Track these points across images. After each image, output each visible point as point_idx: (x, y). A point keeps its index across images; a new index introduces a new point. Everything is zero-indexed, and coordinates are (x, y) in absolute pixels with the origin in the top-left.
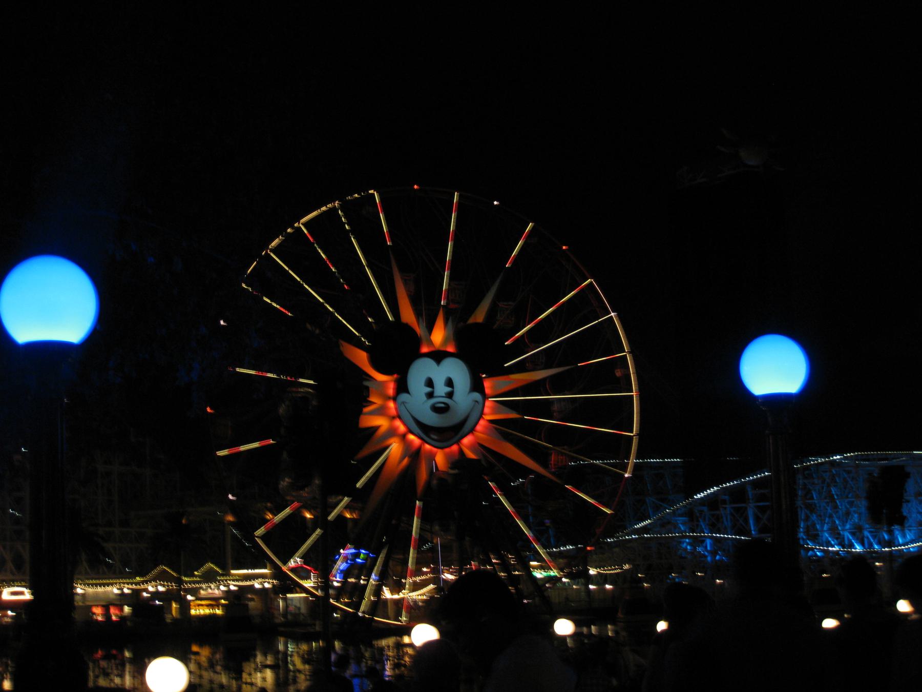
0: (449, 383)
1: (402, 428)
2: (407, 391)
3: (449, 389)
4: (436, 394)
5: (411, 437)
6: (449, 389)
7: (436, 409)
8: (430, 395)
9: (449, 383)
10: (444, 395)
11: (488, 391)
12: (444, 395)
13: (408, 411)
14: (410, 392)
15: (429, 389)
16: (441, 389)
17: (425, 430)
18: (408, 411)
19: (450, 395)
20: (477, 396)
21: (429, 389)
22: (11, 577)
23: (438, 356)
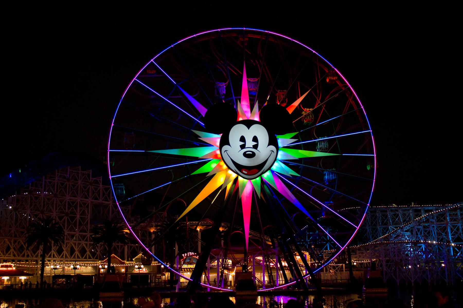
0: (255, 139)
1: (225, 167)
3: (255, 143)
4: (246, 147)
5: (230, 172)
6: (255, 143)
7: (245, 155)
8: (243, 147)
9: (255, 139)
11: (280, 145)
13: (228, 155)
15: (243, 143)
16: (250, 143)
17: (239, 168)
18: (228, 155)
19: (256, 147)
20: (272, 148)
21: (243, 143)
22: (13, 258)
23: (249, 123)
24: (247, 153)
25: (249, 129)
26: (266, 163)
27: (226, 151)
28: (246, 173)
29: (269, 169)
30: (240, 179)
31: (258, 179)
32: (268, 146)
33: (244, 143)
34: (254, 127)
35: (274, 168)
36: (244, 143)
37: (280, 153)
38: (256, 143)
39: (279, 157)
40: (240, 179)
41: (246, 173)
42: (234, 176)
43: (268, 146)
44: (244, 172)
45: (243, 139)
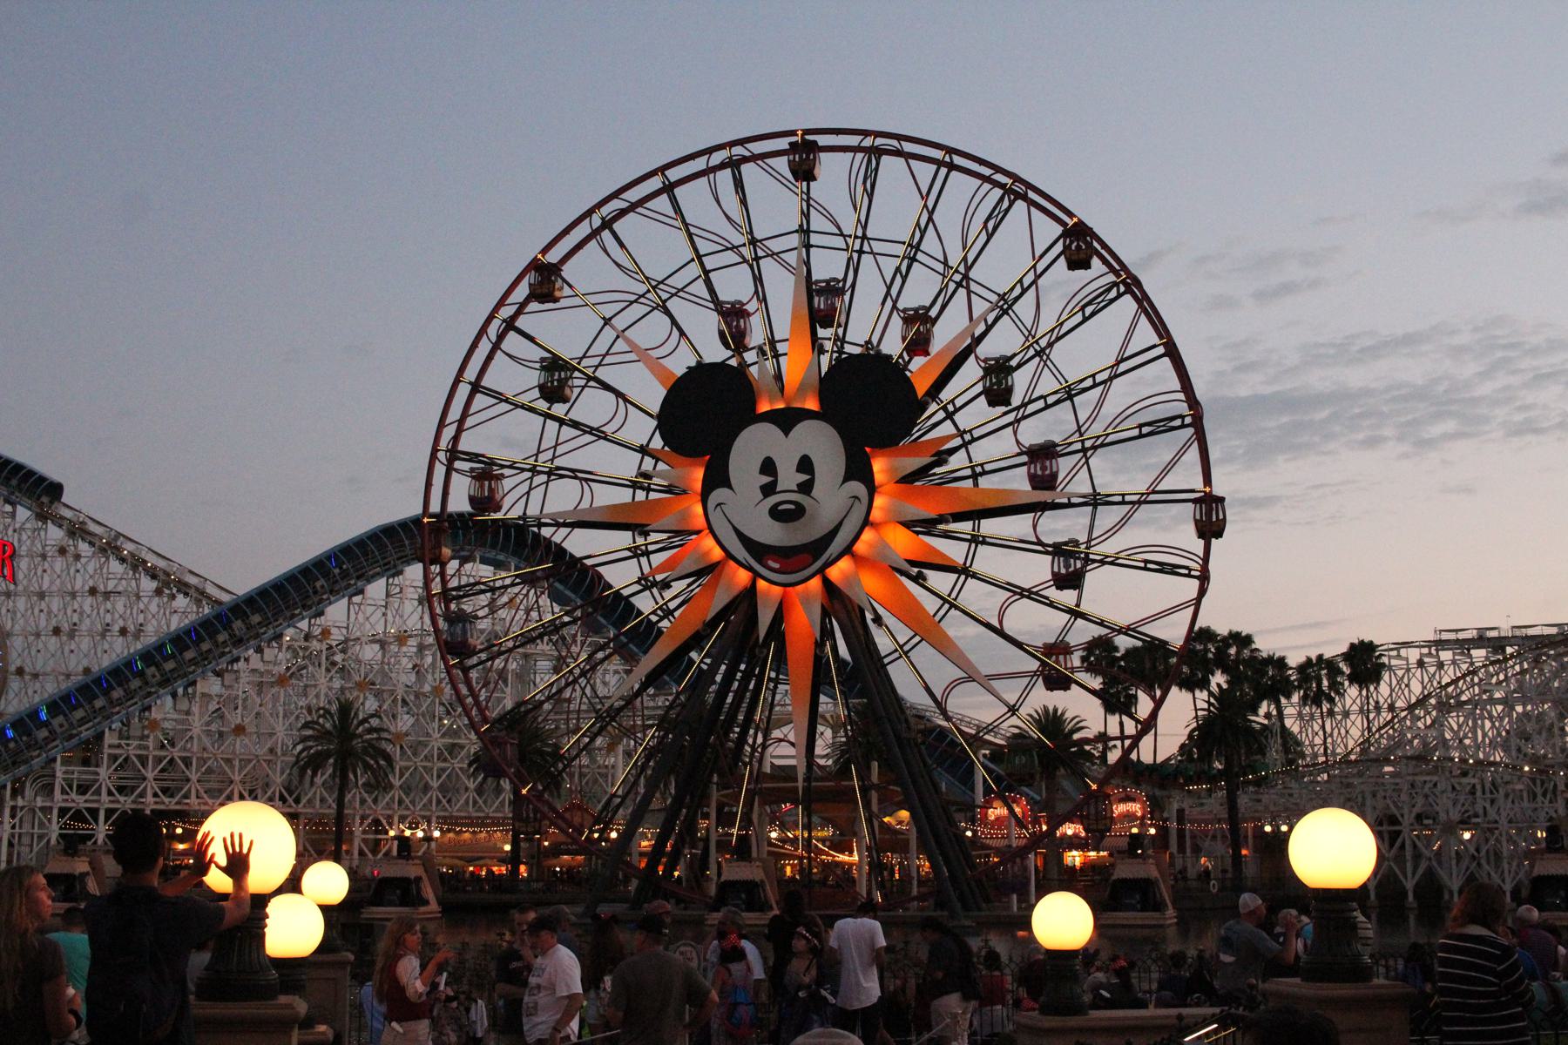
0: (805, 465)
1: (718, 553)
2: (730, 487)
3: (804, 477)
4: (778, 490)
6: (806, 477)
7: (775, 513)
8: (768, 490)
9: (805, 465)
10: (796, 489)
12: (796, 489)
14: (733, 486)
15: (766, 479)
16: (789, 478)
17: (759, 551)
19: (806, 488)
20: (857, 487)
21: (766, 479)
23: (787, 420)
24: (780, 508)
25: (787, 434)
26: (832, 541)
27: (719, 504)
28: (776, 566)
29: (848, 550)
30: (761, 584)
31: (815, 583)
32: (844, 482)
33: (770, 479)
34: (803, 429)
35: (860, 547)
36: (770, 479)
37: (879, 501)
38: (806, 477)
39: (876, 514)
40: (761, 584)
41: (776, 566)
42: (743, 576)
43: (844, 482)
44: (772, 564)
45: (768, 467)
